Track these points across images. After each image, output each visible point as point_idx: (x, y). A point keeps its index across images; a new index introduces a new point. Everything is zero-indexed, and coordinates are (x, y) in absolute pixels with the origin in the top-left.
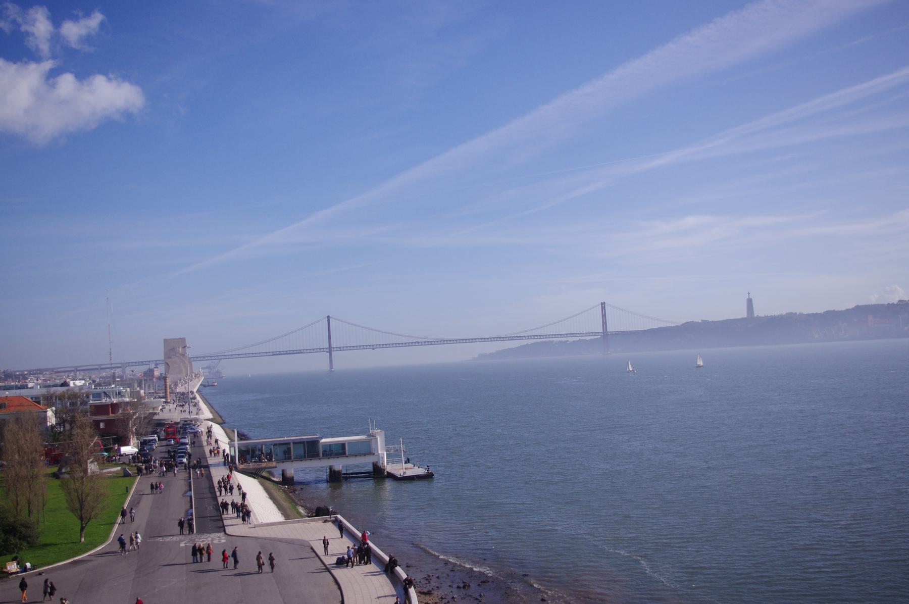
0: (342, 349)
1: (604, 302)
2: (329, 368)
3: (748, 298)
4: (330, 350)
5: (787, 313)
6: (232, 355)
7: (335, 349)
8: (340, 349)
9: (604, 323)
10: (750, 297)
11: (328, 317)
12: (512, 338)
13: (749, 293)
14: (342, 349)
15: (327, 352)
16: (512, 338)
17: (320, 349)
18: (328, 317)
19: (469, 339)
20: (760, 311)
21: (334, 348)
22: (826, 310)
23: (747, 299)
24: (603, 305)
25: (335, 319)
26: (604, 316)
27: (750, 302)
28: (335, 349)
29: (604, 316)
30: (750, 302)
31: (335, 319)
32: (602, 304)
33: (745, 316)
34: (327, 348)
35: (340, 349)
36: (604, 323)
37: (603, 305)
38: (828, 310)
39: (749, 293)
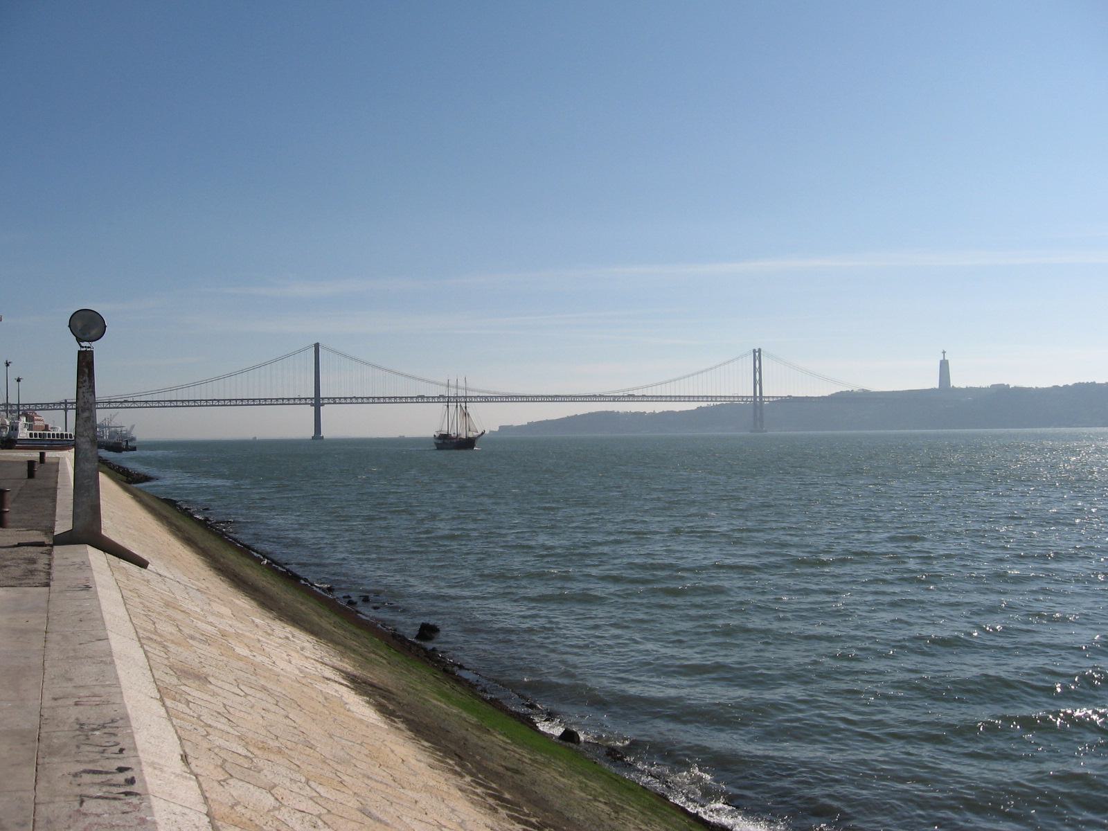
0: (337, 401)
1: (760, 350)
2: (309, 433)
3: (942, 359)
4: (317, 402)
5: (992, 385)
6: (147, 402)
7: (326, 401)
8: (334, 401)
9: (758, 382)
10: (946, 359)
11: (317, 346)
12: (615, 399)
13: (944, 352)
14: (337, 401)
15: (312, 405)
16: (615, 399)
17: (300, 399)
18: (317, 346)
19: (547, 397)
20: (957, 381)
21: (323, 399)
22: (1074, 383)
23: (941, 361)
24: (757, 354)
25: (328, 349)
26: (757, 370)
27: (944, 365)
28: (326, 401)
29: (757, 370)
30: (944, 365)
31: (328, 349)
32: (754, 351)
33: (937, 387)
34: (311, 399)
35: (334, 401)
36: (758, 382)
37: (757, 354)
38: (1077, 382)
39: (944, 352)
